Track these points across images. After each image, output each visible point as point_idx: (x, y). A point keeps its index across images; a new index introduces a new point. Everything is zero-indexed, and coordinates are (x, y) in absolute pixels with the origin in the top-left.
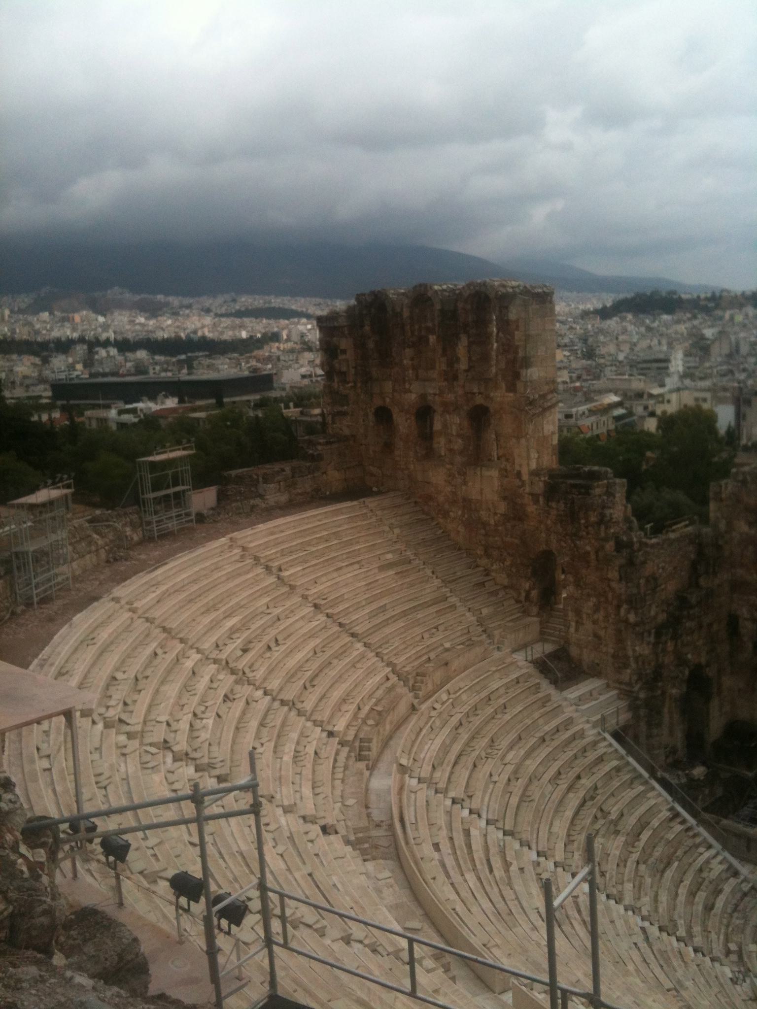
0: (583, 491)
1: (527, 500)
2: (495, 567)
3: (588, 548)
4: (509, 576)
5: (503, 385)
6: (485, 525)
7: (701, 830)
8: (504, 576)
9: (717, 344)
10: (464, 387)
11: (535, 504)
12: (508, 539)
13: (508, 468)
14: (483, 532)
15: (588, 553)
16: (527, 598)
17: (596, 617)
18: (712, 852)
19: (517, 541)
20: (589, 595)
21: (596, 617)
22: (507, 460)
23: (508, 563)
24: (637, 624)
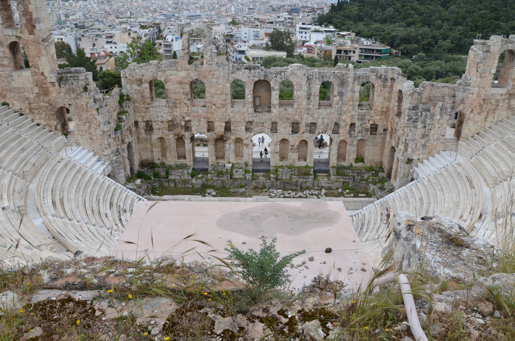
0: (76, 78)
1: (49, 85)
2: (37, 118)
3: (83, 103)
4: (45, 120)
6: (27, 99)
8: (43, 121)
11: (53, 87)
12: (42, 104)
13: (36, 71)
14: (27, 102)
15: (82, 105)
16: (56, 129)
17: (90, 131)
20: (85, 123)
21: (90, 131)
22: (35, 67)
23: (43, 115)
24: (108, 131)
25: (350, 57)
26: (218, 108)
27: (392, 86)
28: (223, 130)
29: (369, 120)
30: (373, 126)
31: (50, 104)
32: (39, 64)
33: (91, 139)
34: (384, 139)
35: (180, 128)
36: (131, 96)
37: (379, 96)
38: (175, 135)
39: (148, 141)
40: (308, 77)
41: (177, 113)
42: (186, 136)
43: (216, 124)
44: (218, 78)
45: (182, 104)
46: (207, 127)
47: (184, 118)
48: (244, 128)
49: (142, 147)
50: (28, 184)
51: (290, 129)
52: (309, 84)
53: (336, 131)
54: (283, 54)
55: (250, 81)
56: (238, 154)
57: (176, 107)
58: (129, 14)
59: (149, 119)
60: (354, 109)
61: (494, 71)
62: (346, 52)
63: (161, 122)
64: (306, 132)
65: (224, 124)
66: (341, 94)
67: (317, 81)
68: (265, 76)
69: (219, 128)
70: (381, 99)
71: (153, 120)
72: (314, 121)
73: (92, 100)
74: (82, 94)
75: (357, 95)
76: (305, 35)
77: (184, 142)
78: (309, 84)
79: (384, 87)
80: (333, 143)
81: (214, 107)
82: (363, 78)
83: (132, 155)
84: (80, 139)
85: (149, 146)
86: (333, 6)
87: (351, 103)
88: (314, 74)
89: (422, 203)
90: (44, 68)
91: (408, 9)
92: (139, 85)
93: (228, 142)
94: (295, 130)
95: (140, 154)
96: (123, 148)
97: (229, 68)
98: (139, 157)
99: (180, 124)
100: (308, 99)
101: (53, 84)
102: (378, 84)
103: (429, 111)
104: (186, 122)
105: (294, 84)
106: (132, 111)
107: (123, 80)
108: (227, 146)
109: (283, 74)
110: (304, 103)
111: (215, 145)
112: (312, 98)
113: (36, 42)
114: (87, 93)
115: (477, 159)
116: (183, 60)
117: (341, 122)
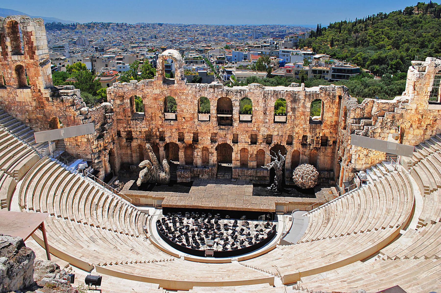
2: (34, 126)
5: (28, 56)
6: (27, 111)
7: (123, 200)
9: (78, 41)
10: (11, 58)
12: (38, 115)
13: (35, 88)
18: (127, 205)
19: (42, 116)
22: (33, 85)
23: (39, 124)
25: (324, 77)
26: (188, 121)
27: (339, 103)
28: (192, 140)
29: (319, 133)
30: (323, 138)
31: (45, 115)
32: (37, 82)
33: (77, 145)
34: (334, 149)
35: (155, 138)
36: (114, 109)
39: (129, 148)
40: (264, 95)
42: (161, 145)
43: (186, 135)
44: (187, 95)
45: (158, 118)
46: (178, 137)
47: (158, 129)
48: (209, 138)
49: (124, 152)
50: (17, 181)
51: (249, 141)
52: (265, 102)
53: (290, 143)
54: (265, 73)
55: (214, 98)
57: (152, 120)
58: (141, 40)
59: (129, 130)
61: (430, 89)
62: (320, 72)
63: (140, 132)
64: (263, 142)
65: (192, 135)
66: (293, 109)
67: (272, 99)
68: (227, 94)
69: (189, 138)
70: (330, 114)
72: (269, 133)
73: (79, 112)
74: (70, 107)
75: (308, 110)
76: (287, 58)
77: (159, 149)
78: (265, 102)
79: (333, 103)
81: (184, 120)
82: (313, 96)
83: (114, 160)
84: (68, 144)
85: (129, 152)
86: (312, 33)
87: (303, 117)
88: (269, 92)
89: (359, 209)
90: (40, 86)
91: (379, 34)
92: (121, 101)
94: (254, 142)
95: (121, 158)
96: (104, 153)
97: (196, 87)
98: (120, 160)
99: (156, 133)
100: (264, 114)
101: (47, 99)
102: (326, 101)
103: (371, 125)
104: (160, 132)
105: (252, 101)
106: (115, 123)
107: (108, 96)
108: (195, 154)
109: (242, 92)
110: (261, 118)
112: (268, 114)
113: (35, 64)
114: (75, 107)
115: (414, 169)
116: (157, 80)
117: (294, 134)
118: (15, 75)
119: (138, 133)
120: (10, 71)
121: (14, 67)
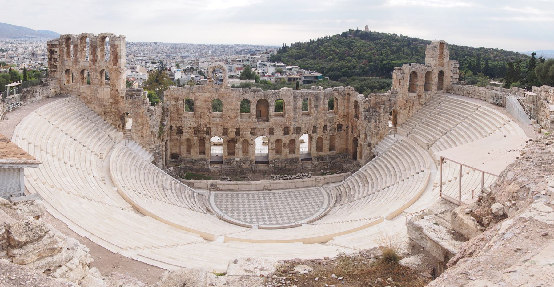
37: (341, 106)
38: (199, 137)
41: (202, 122)
47: (206, 125)
51: (283, 132)
53: (314, 131)
56: (245, 151)
60: (325, 116)
64: (294, 133)
66: (316, 106)
71: (183, 126)
72: (299, 126)
75: (327, 106)
79: (344, 99)
80: (313, 140)
87: (323, 112)
93: (238, 143)
94: (286, 131)
104: (207, 128)
108: (237, 145)
111: (228, 145)
118: (99, 77)
119: (188, 128)
120: (96, 74)
121: (99, 70)
